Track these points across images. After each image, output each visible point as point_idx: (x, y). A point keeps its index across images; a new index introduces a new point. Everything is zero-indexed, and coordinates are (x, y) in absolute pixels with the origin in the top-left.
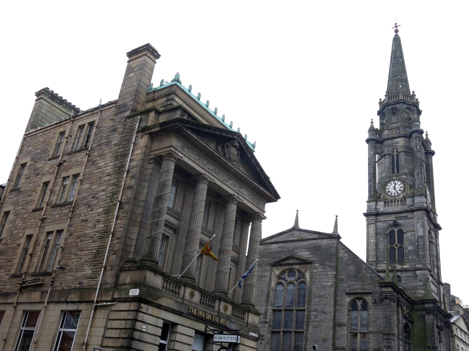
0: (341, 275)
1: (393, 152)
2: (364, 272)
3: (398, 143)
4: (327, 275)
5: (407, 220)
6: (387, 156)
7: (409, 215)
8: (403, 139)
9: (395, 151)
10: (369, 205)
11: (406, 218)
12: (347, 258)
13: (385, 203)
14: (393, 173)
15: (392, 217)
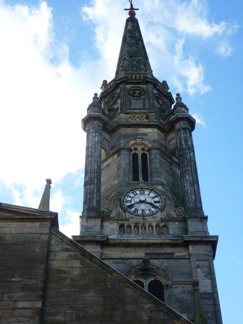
0: (57, 314)
1: (136, 149)
2: (130, 308)
3: (146, 134)
4: (14, 309)
5: (171, 262)
6: (124, 152)
7: (179, 252)
8: (155, 130)
9: (139, 148)
10: (86, 224)
11: (170, 257)
12: (76, 273)
13: (122, 226)
14: (136, 178)
15: (141, 253)
